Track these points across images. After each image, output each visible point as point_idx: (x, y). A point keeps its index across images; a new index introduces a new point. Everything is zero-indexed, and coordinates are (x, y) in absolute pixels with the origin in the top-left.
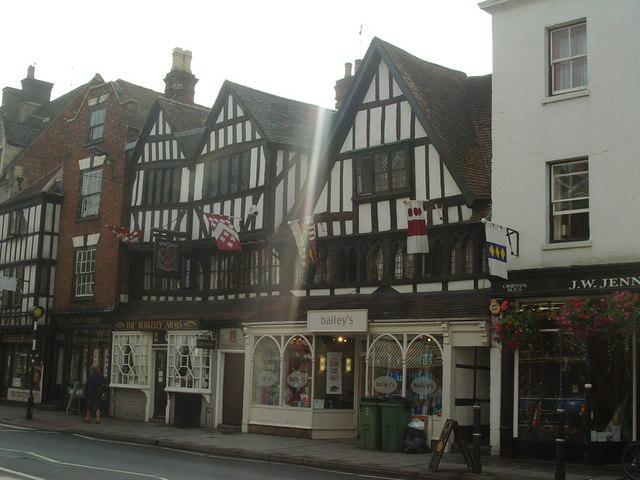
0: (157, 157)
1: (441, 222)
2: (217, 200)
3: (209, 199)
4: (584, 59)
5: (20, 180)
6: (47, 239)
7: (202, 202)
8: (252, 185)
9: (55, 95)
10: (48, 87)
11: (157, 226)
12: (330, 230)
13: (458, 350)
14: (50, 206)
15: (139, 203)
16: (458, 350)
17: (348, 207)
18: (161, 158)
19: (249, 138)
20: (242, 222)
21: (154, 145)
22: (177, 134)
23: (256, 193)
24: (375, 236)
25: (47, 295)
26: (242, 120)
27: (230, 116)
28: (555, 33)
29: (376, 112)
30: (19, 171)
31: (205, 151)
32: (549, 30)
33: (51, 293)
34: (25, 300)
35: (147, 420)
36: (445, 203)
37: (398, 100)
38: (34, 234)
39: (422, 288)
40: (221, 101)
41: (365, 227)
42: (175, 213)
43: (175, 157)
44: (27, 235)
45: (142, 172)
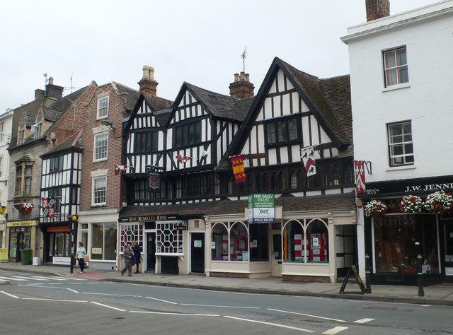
0: (138, 126)
2: (181, 149)
3: (176, 147)
4: (406, 68)
5: (54, 140)
6: (75, 172)
7: (172, 150)
8: (203, 140)
9: (65, 93)
10: (60, 89)
11: (149, 163)
12: (251, 163)
13: (337, 227)
14: (76, 154)
15: (132, 152)
16: (337, 227)
17: (262, 150)
18: (145, 126)
19: (200, 114)
20: (198, 161)
21: (140, 119)
22: (155, 113)
23: (206, 144)
24: (279, 166)
25: (76, 204)
26: (195, 104)
27: (188, 103)
28: (387, 54)
29: (277, 99)
30: (53, 135)
31: (172, 122)
32: (383, 52)
33: (78, 203)
34: (63, 207)
35: (143, 272)
36: (321, 148)
37: (290, 92)
38: (67, 170)
39: (309, 194)
40: (181, 94)
41: (273, 161)
42: (155, 156)
43: (154, 125)
44: (63, 171)
45: (133, 134)
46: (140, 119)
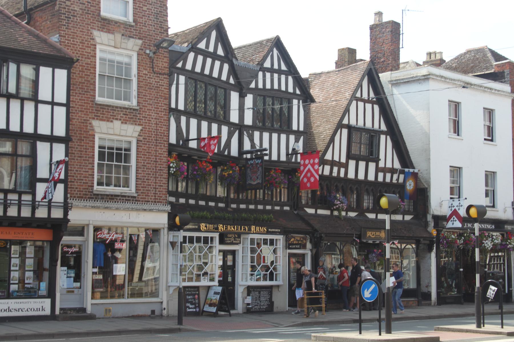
1: (396, 182)
17: (343, 160)
20: (288, 154)
36: (393, 171)
41: (351, 175)
43: (224, 78)
46: (200, 58)
